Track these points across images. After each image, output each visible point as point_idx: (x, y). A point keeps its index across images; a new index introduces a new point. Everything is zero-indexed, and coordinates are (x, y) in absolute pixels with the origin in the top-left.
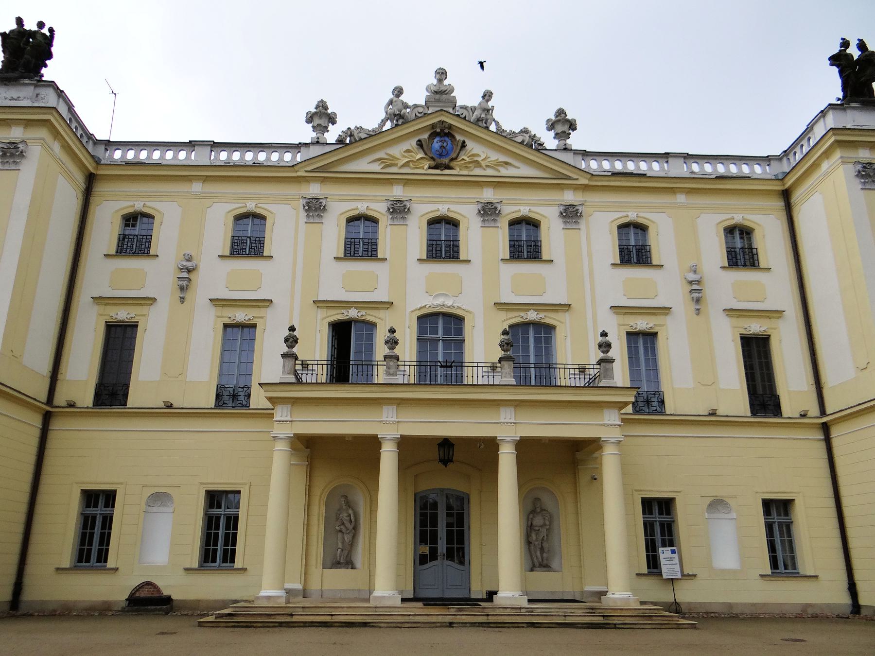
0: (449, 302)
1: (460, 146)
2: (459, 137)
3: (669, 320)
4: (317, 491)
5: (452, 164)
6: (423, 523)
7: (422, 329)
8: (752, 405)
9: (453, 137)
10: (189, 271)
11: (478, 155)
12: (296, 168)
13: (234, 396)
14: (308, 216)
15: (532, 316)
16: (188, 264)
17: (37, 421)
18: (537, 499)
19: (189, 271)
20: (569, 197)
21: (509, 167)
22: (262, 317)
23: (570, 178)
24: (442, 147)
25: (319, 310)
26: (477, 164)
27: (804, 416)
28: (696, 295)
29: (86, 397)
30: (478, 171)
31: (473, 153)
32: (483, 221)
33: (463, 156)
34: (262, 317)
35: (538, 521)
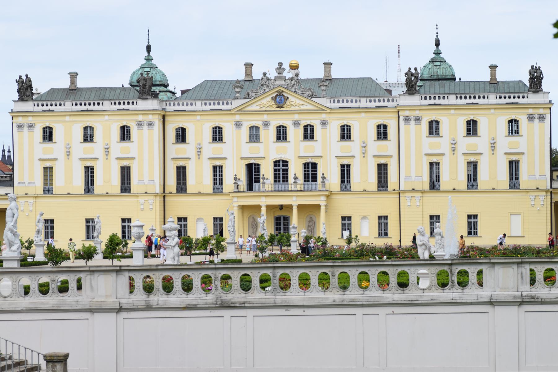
0: (283, 157)
1: (286, 99)
2: (285, 95)
3: (354, 160)
4: (245, 217)
5: (284, 106)
6: (277, 225)
7: (275, 166)
8: (378, 187)
9: (284, 95)
10: (200, 149)
11: (293, 102)
12: (231, 111)
13: (218, 189)
14: (236, 128)
15: (310, 160)
16: (199, 147)
17: (162, 199)
18: (311, 217)
19: (200, 149)
20: (324, 116)
21: (304, 106)
22: (224, 163)
23: (325, 110)
24: (280, 100)
25: (242, 161)
26: (292, 105)
27: (394, 190)
28: (364, 152)
29: (174, 190)
30: (293, 108)
31: (291, 101)
32: (295, 127)
33: (287, 103)
34: (224, 163)
35: (311, 224)
